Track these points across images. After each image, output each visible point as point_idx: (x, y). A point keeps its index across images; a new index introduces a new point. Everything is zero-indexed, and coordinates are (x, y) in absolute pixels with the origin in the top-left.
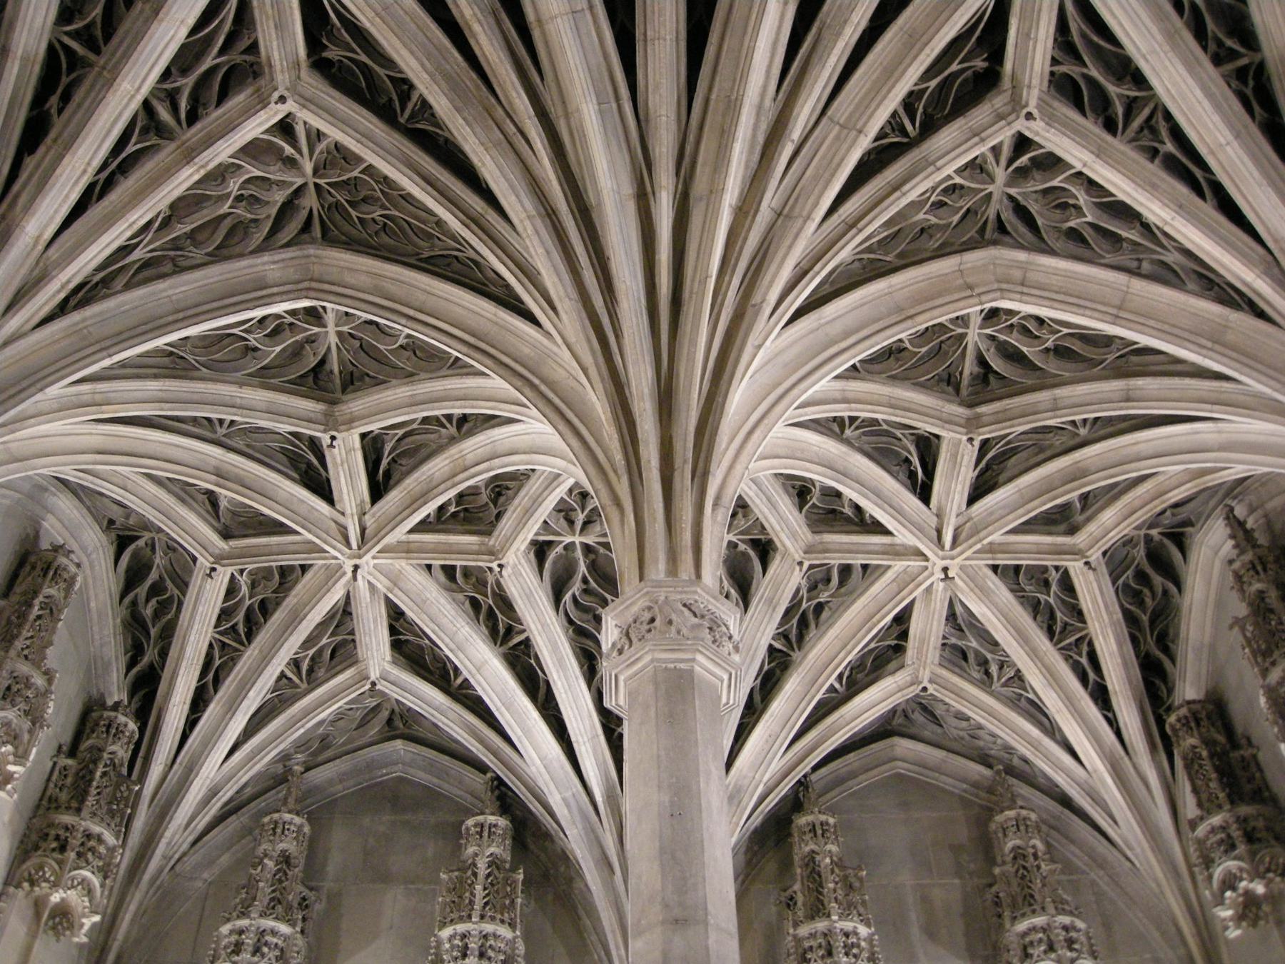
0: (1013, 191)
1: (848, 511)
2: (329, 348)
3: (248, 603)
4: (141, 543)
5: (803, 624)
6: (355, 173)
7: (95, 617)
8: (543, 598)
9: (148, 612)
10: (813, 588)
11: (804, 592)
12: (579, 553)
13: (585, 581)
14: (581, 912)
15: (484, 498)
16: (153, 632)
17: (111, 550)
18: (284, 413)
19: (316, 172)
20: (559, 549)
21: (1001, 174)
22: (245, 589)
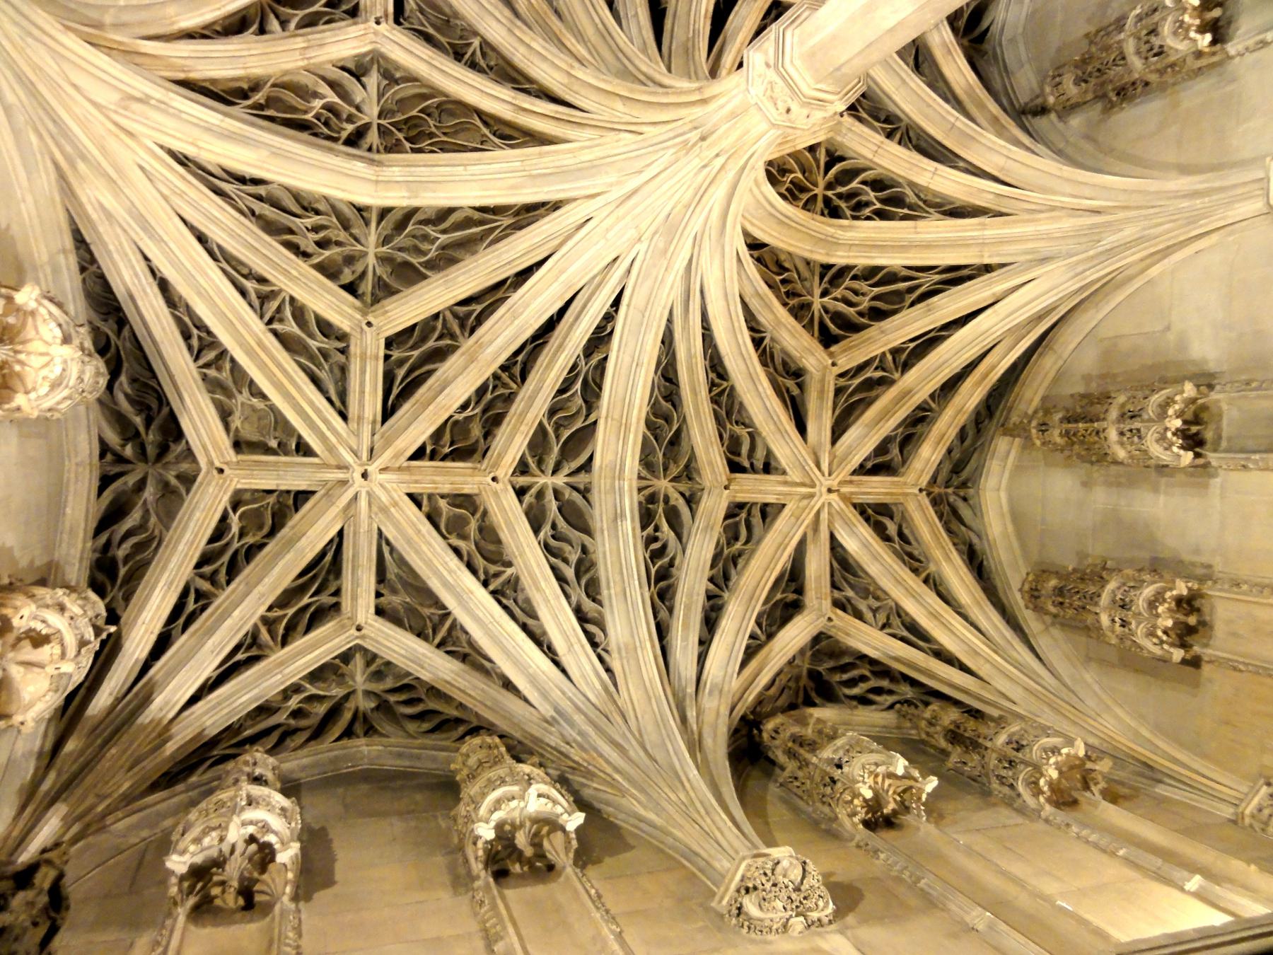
0: (830, 193)
1: (746, 464)
2: (364, 274)
3: (236, 545)
4: (131, 480)
5: (727, 578)
6: (414, 113)
7: (67, 525)
8: (524, 526)
9: (121, 553)
10: (729, 544)
11: (723, 540)
12: (550, 495)
13: (554, 526)
14: (602, 806)
15: (476, 431)
16: (122, 571)
17: (96, 484)
18: (327, 301)
19: (379, 117)
20: (533, 491)
21: (822, 183)
22: (235, 529)
